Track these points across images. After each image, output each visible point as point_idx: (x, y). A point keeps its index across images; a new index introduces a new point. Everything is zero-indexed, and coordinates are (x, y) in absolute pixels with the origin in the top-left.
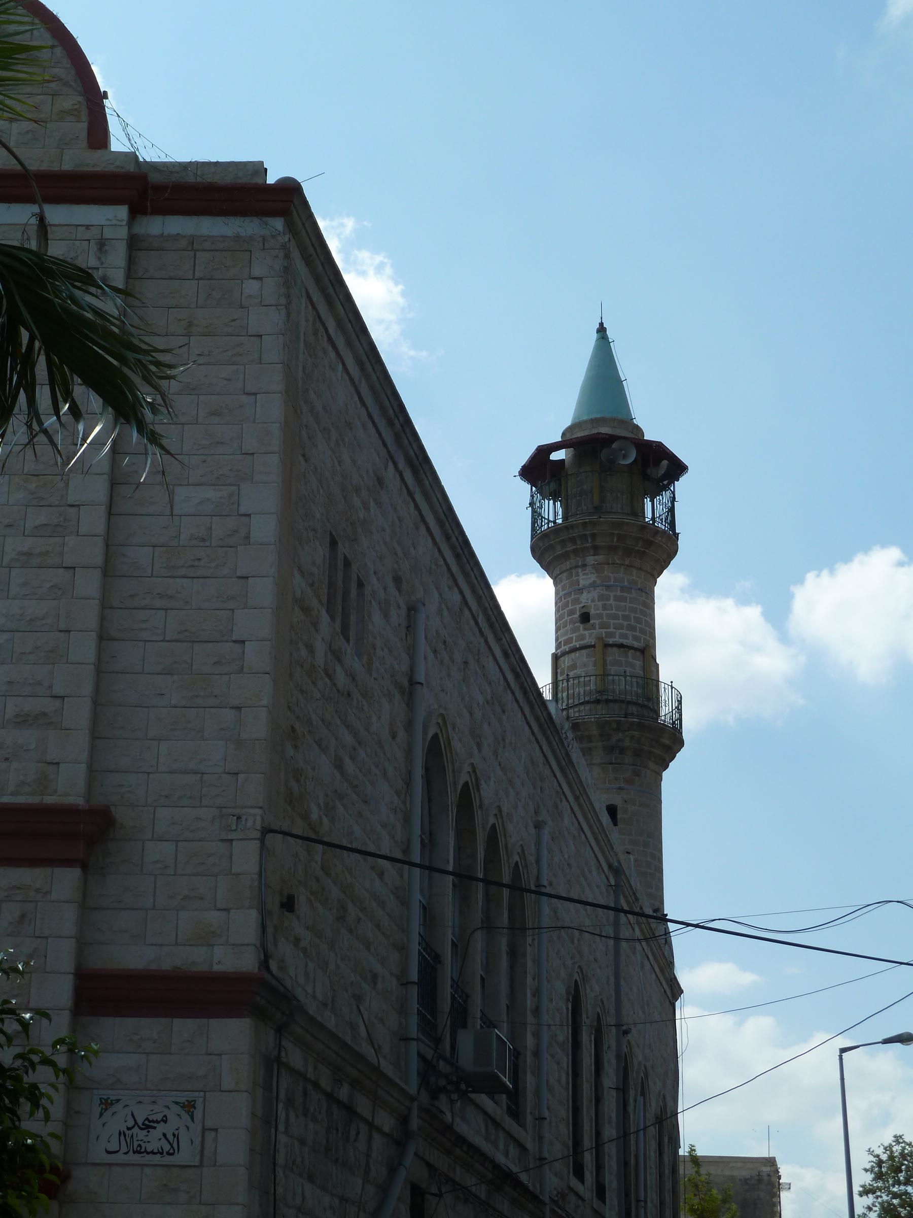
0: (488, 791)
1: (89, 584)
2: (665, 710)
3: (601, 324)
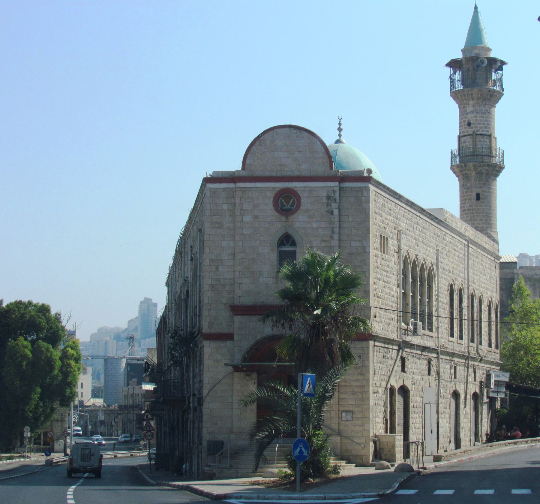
3: (476, 5)
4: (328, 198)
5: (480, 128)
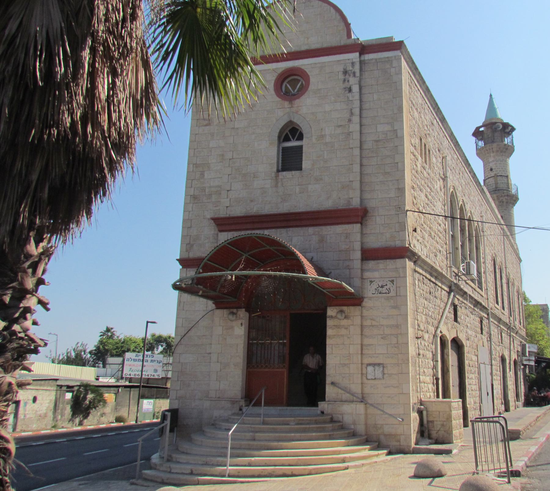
0: (468, 207)
1: (357, 152)
2: (513, 192)
4: (345, 72)
5: (500, 171)
